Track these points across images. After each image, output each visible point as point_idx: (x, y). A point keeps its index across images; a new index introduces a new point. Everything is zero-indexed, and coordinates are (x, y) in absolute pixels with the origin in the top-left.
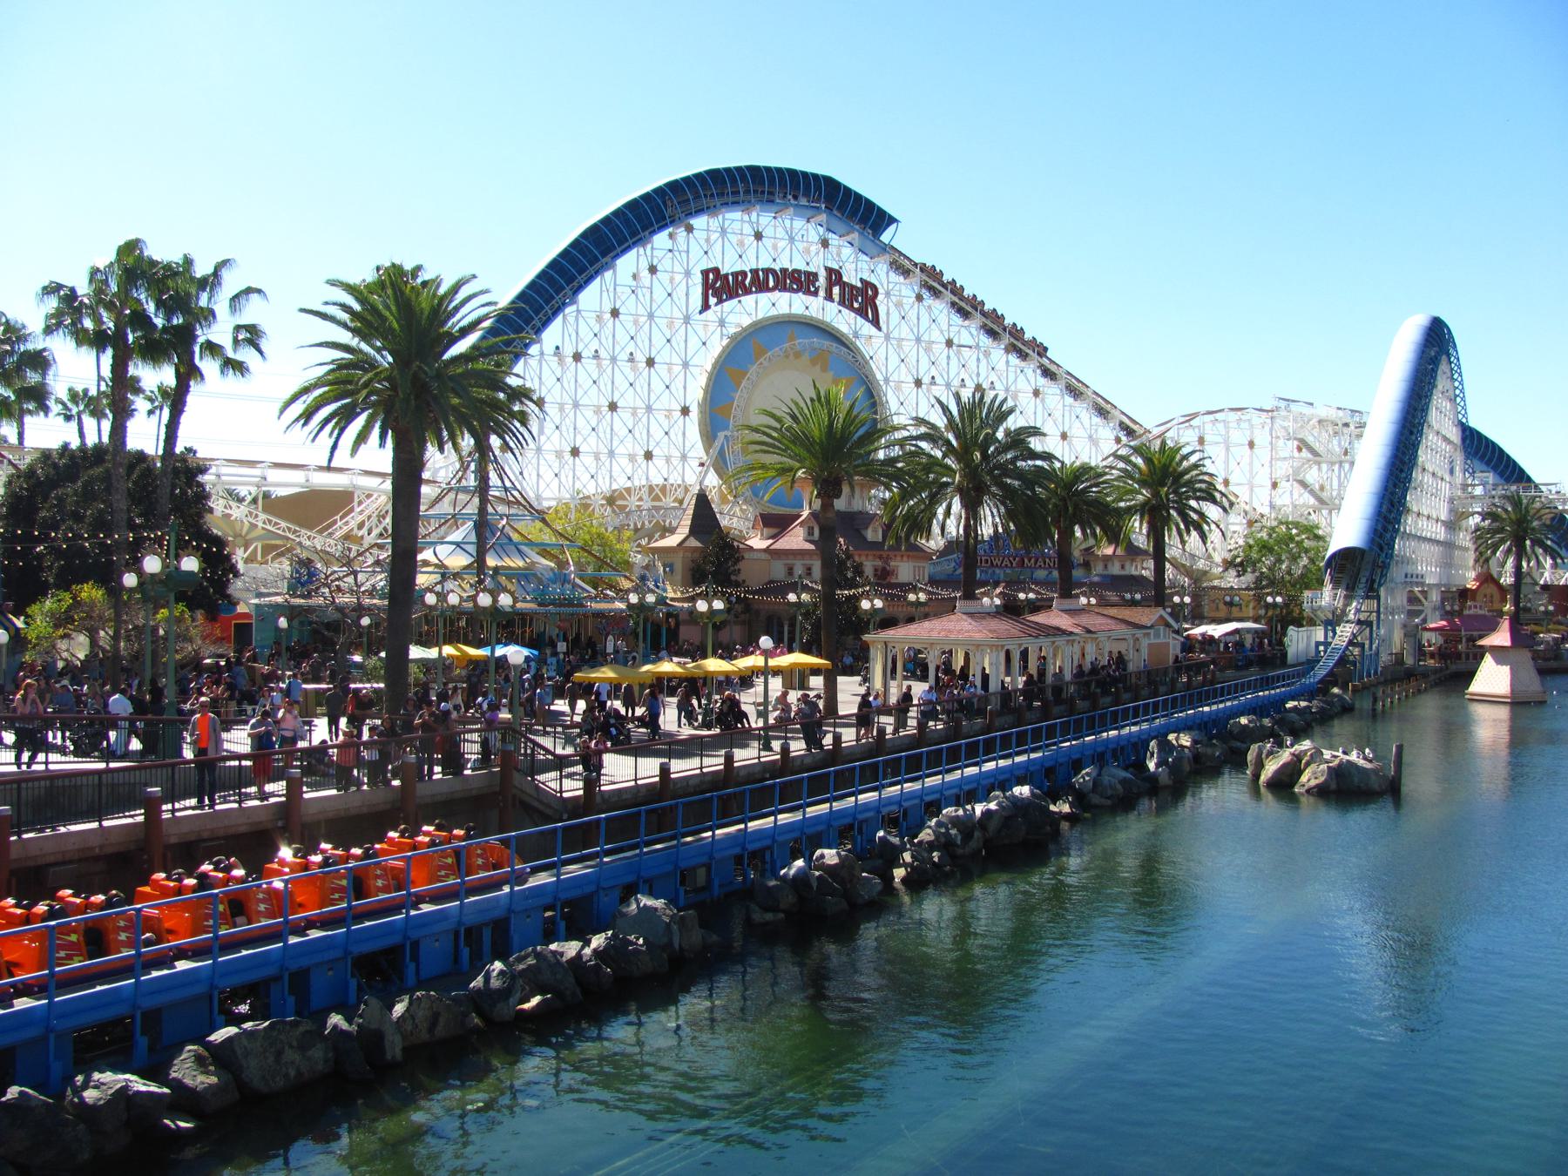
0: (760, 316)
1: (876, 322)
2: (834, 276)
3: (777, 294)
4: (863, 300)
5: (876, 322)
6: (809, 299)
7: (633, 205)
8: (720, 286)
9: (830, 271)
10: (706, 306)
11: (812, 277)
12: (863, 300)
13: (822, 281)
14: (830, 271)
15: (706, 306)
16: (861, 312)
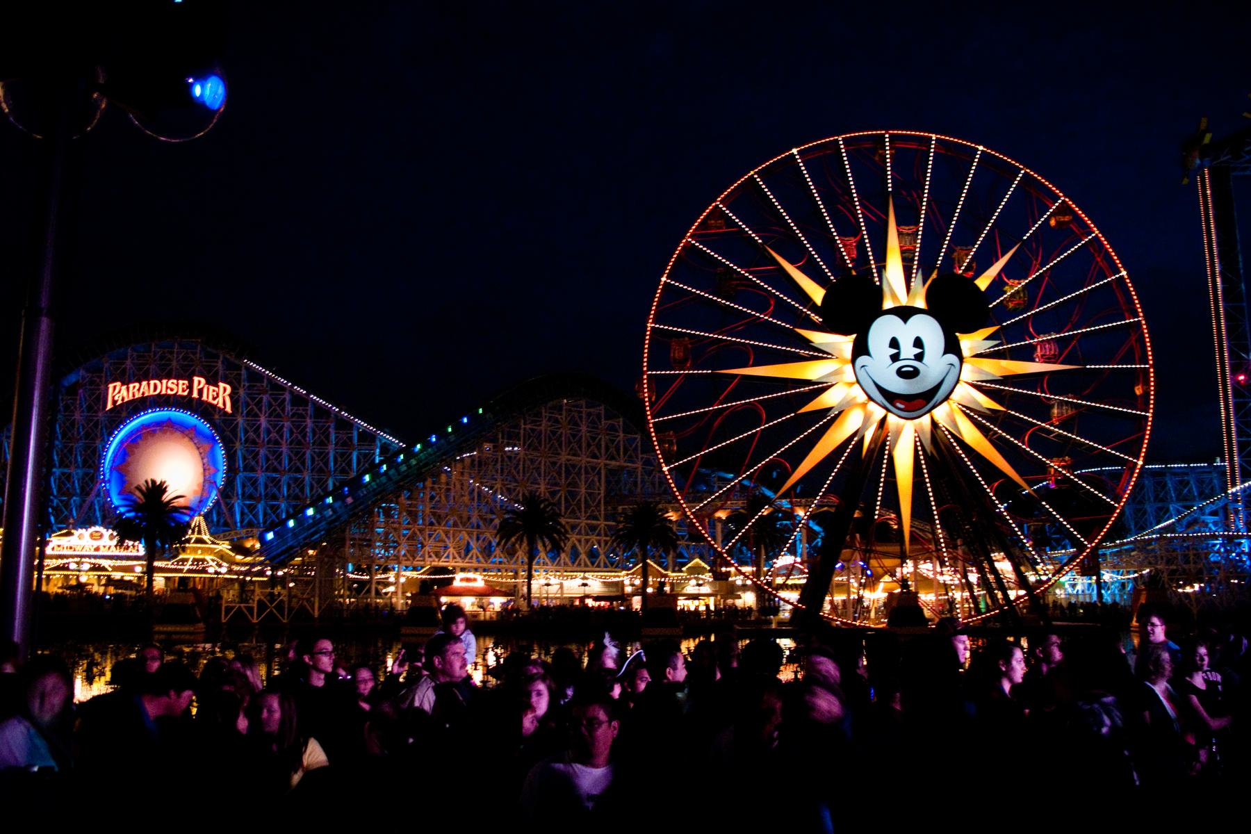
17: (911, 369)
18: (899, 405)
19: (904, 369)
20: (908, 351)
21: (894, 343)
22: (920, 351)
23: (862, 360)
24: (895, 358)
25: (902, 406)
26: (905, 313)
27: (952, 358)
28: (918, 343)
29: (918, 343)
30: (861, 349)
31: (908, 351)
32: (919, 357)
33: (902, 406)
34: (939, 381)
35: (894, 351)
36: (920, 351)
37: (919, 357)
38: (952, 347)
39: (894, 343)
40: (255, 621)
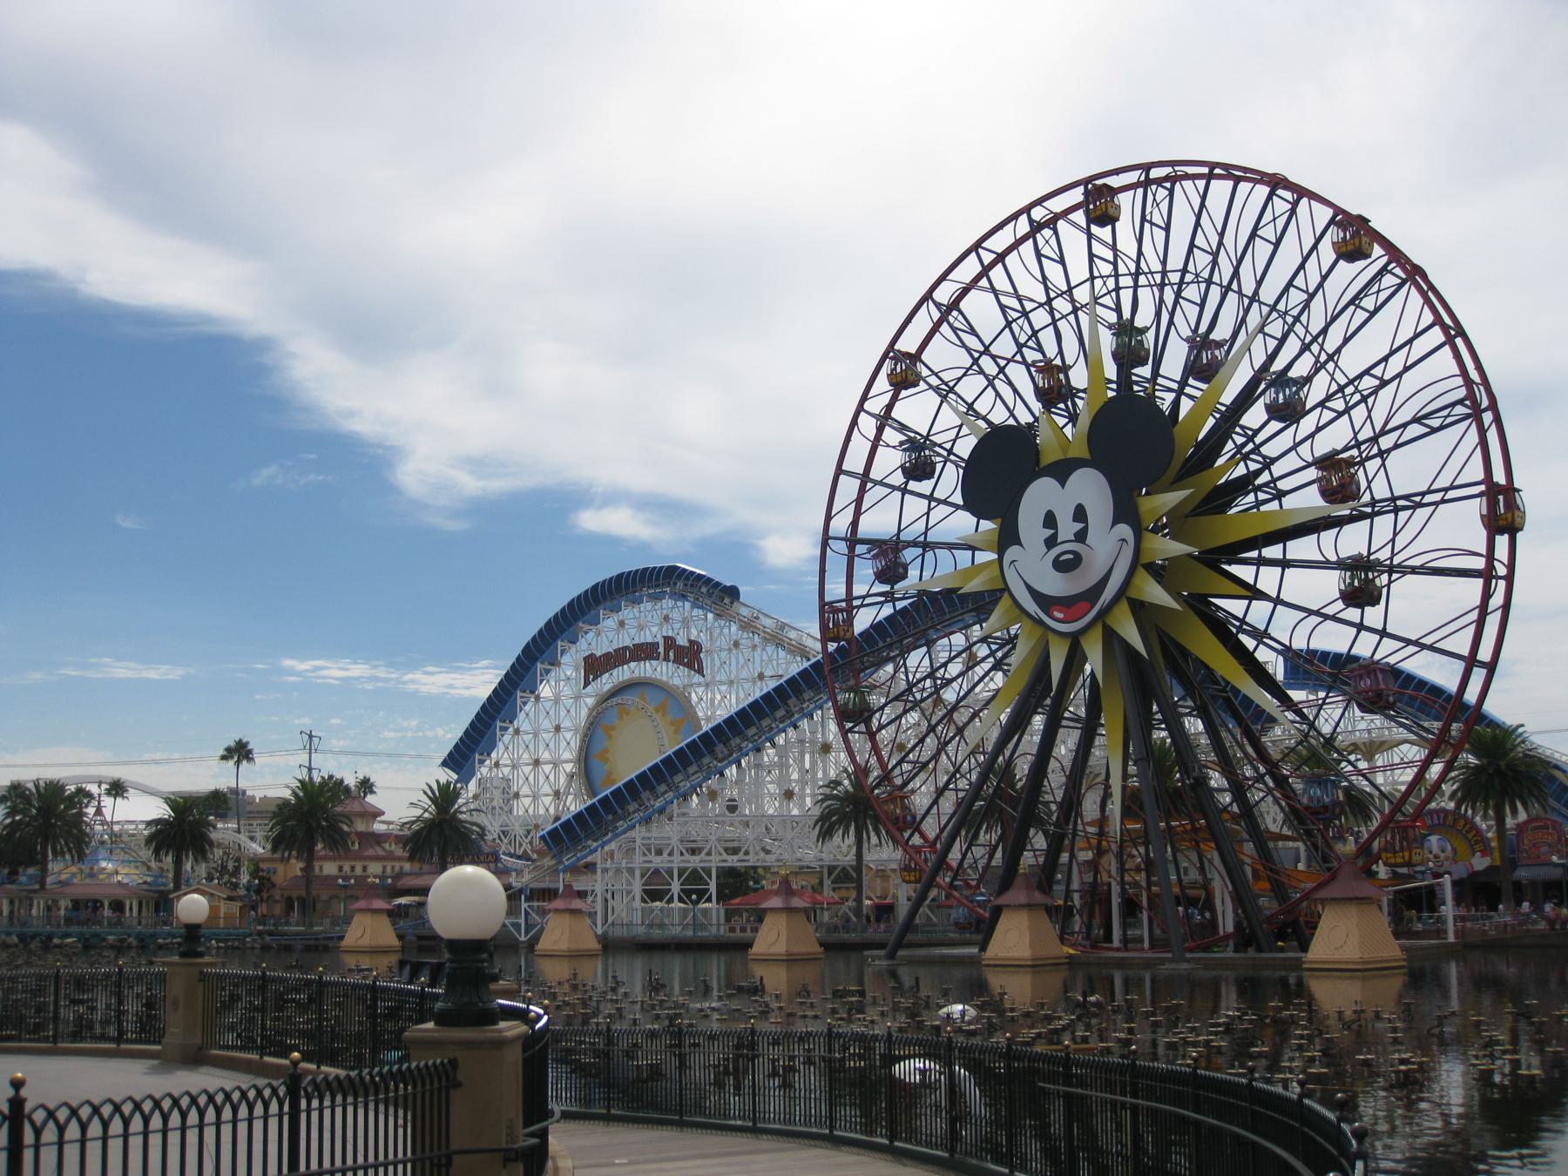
0: (626, 678)
1: (700, 671)
2: (669, 642)
3: (633, 664)
4: (689, 656)
5: (700, 671)
6: (654, 663)
7: (548, 624)
8: (595, 666)
9: (666, 638)
10: (587, 683)
11: (655, 645)
12: (689, 656)
13: (661, 650)
14: (666, 638)
15: (587, 683)
16: (690, 666)
17: (1071, 556)
18: (1057, 614)
19: (1061, 559)
20: (1067, 528)
21: (1050, 520)
22: (1082, 525)
23: (1012, 552)
24: (1051, 542)
25: (1060, 616)
26: (1062, 471)
27: (1125, 530)
28: (1080, 514)
29: (1080, 514)
30: (1008, 537)
31: (1067, 528)
32: (1081, 536)
33: (1060, 616)
34: (1106, 570)
35: (1050, 532)
36: (1082, 525)
37: (1081, 536)
38: (1125, 511)
39: (1050, 520)
40: (523, 938)
